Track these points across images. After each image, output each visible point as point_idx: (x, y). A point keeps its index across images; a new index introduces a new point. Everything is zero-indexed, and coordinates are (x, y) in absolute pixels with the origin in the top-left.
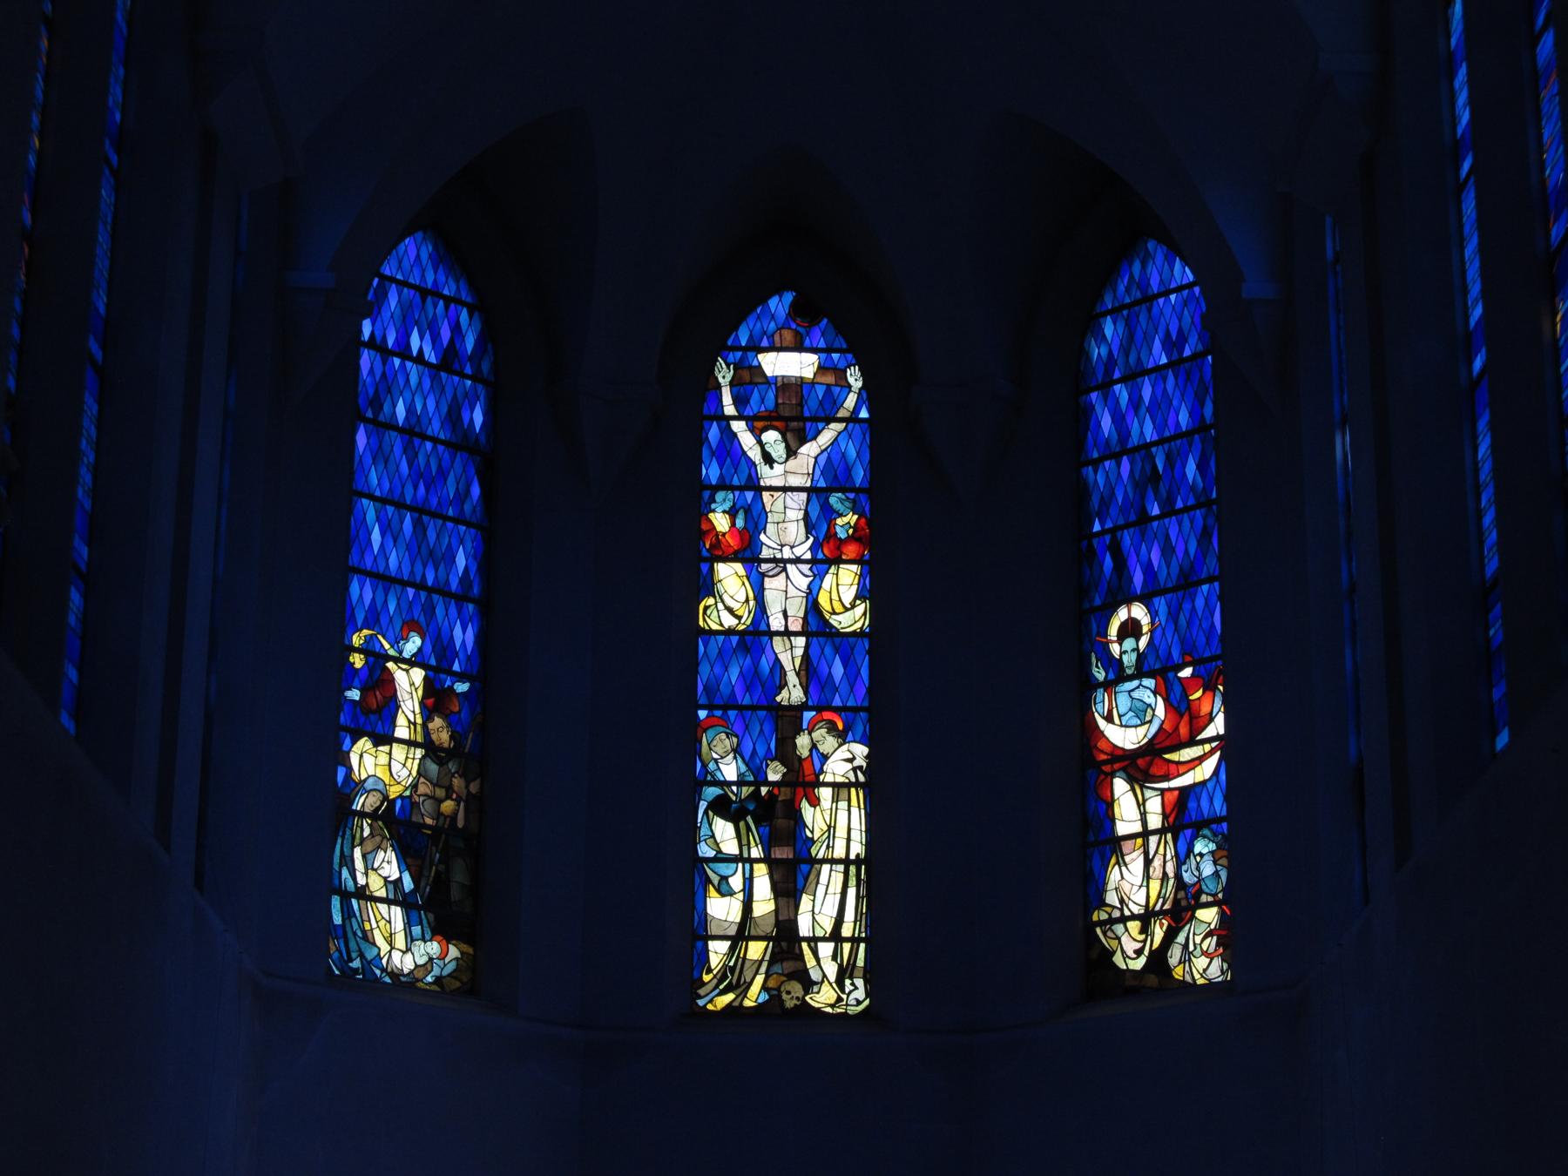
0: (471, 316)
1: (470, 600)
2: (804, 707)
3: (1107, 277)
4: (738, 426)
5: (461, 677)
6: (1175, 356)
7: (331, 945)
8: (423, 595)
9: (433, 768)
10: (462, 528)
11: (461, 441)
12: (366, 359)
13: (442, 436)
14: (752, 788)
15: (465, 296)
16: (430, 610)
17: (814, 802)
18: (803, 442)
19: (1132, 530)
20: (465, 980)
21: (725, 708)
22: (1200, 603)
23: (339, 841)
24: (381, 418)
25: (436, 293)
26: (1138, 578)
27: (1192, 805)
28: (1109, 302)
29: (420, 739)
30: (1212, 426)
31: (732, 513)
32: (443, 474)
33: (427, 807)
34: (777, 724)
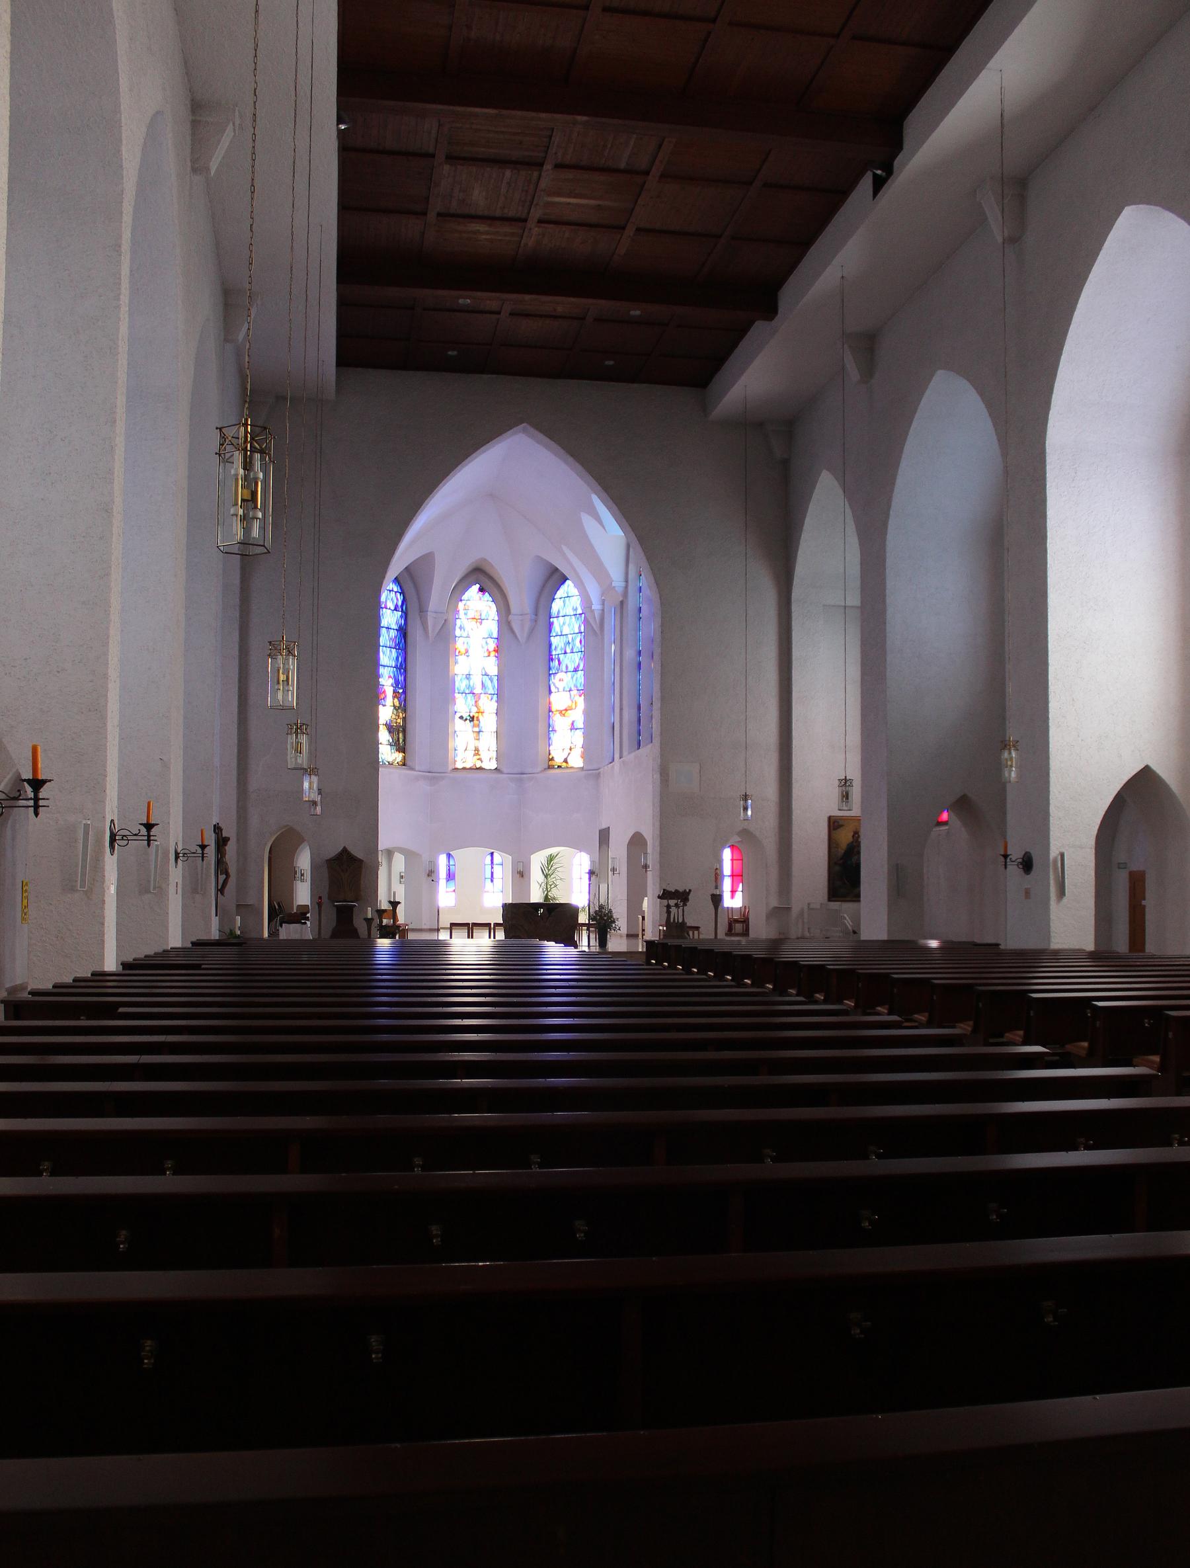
6: (575, 613)
22: (579, 676)
25: (392, 591)
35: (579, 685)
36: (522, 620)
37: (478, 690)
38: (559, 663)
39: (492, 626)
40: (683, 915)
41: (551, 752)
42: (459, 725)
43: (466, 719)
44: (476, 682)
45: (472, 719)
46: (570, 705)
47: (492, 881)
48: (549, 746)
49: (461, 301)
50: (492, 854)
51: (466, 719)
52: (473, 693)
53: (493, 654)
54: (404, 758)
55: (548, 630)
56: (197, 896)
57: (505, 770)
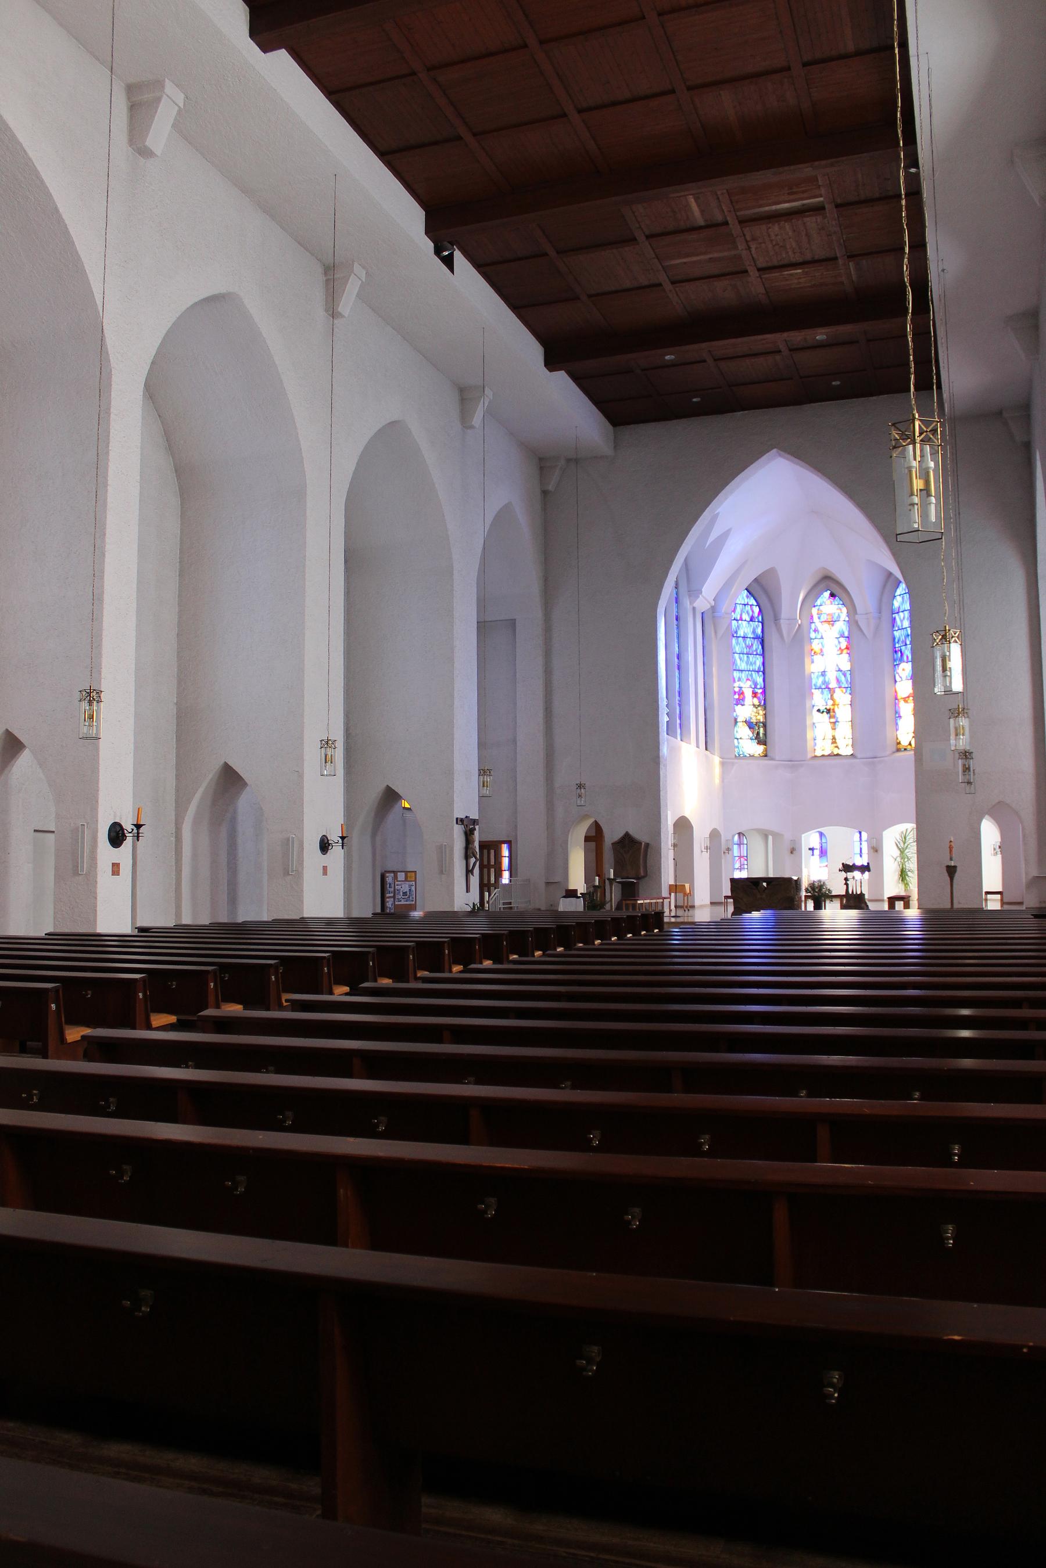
8: (750, 672)
9: (755, 710)
10: (758, 656)
11: (756, 638)
15: (755, 604)
16: (752, 675)
25: (748, 604)
26: (905, 658)
32: (752, 645)
36: (868, 619)
37: (833, 684)
38: (902, 654)
39: (842, 626)
40: (861, 887)
41: (898, 737)
43: (823, 712)
44: (831, 677)
45: (828, 711)
47: (861, 856)
48: (897, 730)
49: (667, 357)
50: (860, 833)
51: (823, 712)
52: (829, 688)
53: (845, 651)
54: (766, 750)
55: (891, 625)
56: (443, 876)
57: (859, 756)
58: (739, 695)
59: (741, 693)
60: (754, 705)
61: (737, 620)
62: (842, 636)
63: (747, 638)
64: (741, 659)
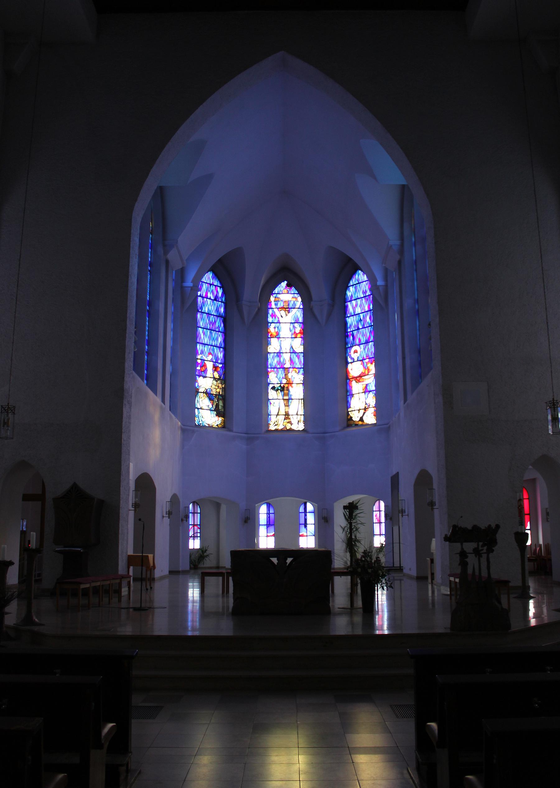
0: (220, 289)
1: (222, 348)
2: (290, 368)
3: (350, 278)
4: (276, 310)
5: (220, 363)
6: (365, 295)
7: (196, 419)
8: (212, 347)
9: (215, 382)
10: (220, 333)
12: (200, 299)
13: (215, 314)
14: (280, 385)
15: (219, 285)
17: (292, 387)
18: (289, 313)
19: (356, 331)
20: (223, 425)
21: (274, 368)
23: (197, 397)
24: (202, 311)
25: (213, 284)
27: (368, 388)
28: (351, 283)
29: (212, 377)
30: (372, 310)
31: (275, 328)
32: (215, 322)
33: (214, 390)
34: (284, 371)
35: (370, 354)
37: (287, 365)
38: (354, 338)
39: (298, 313)
42: (272, 394)
43: (278, 390)
45: (282, 389)
46: (363, 372)
47: (306, 527)
50: (305, 504)
53: (299, 335)
54: (224, 422)
58: (201, 367)
59: (204, 365)
60: (214, 378)
61: (203, 297)
62: (297, 322)
63: (211, 315)
64: (204, 334)
